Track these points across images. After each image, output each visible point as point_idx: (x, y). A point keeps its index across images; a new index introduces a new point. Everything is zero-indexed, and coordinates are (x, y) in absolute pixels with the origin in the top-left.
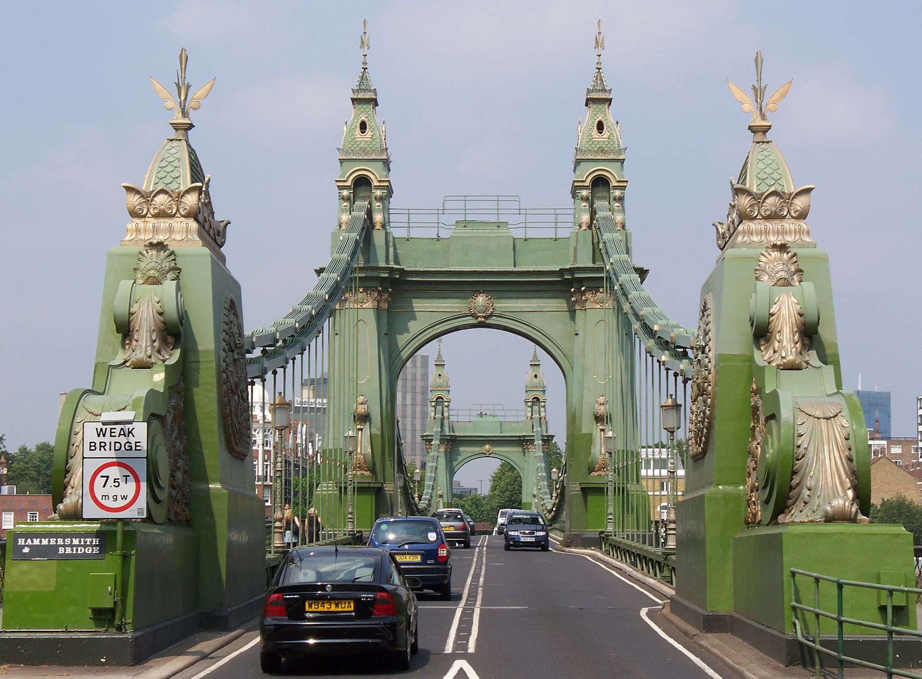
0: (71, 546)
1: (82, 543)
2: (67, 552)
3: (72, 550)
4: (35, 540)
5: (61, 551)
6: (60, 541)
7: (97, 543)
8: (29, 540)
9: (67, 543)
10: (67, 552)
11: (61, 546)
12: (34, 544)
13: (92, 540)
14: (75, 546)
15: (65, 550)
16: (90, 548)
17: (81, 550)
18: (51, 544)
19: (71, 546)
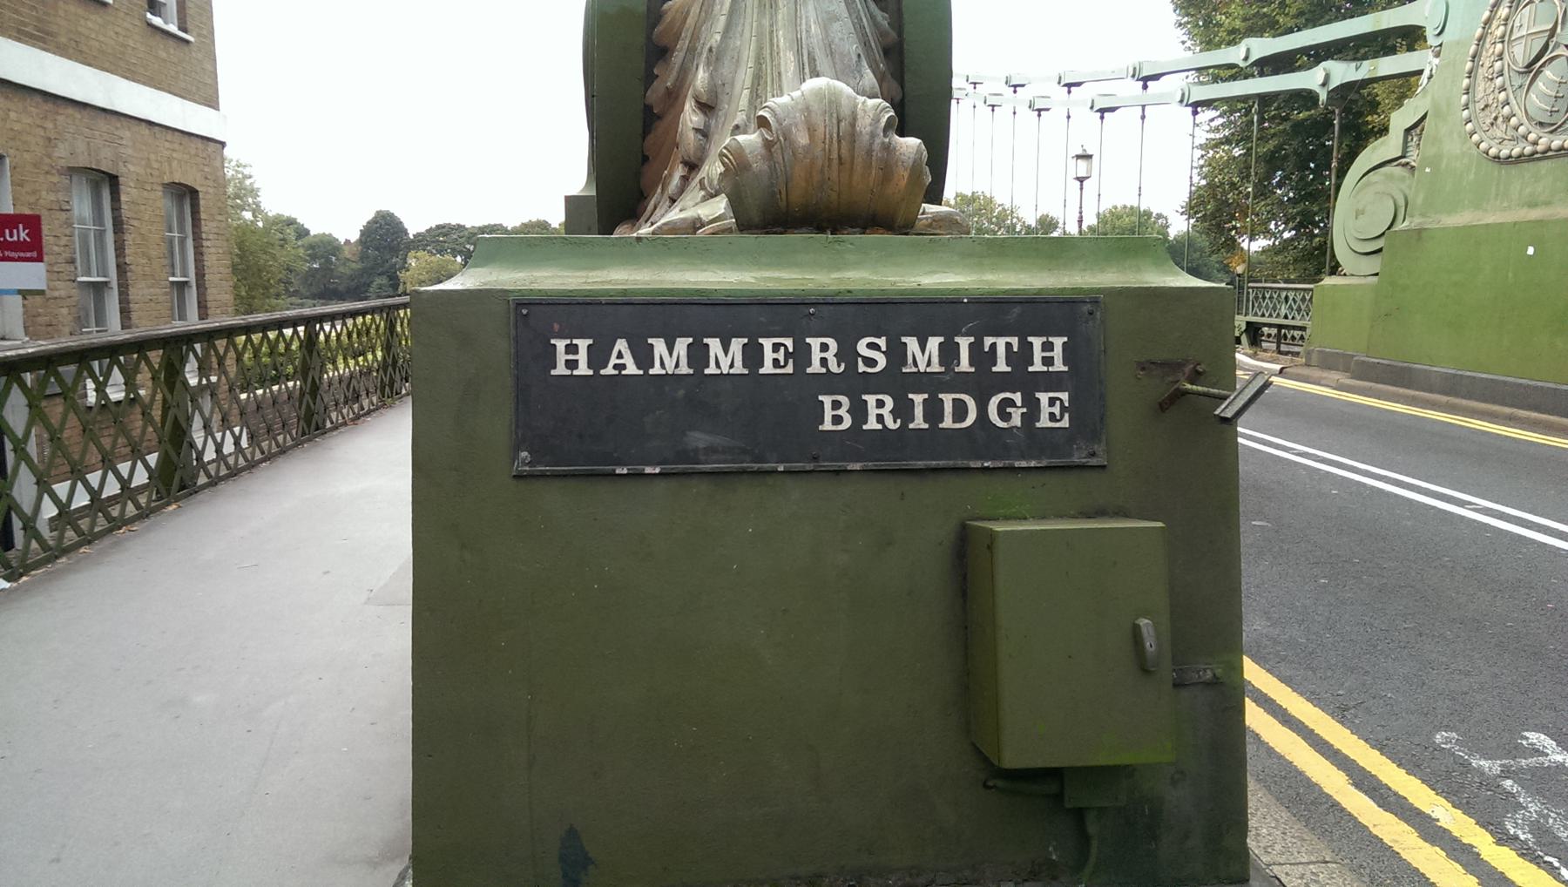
0: (897, 381)
1: (965, 365)
2: (872, 424)
3: (903, 410)
4: (659, 346)
5: (834, 414)
6: (823, 353)
7: (1059, 366)
8: (621, 345)
9: (871, 362)
10: (872, 424)
11: (828, 382)
12: (656, 370)
13: (1027, 348)
14: (923, 381)
15: (859, 411)
16: (1017, 397)
17: (960, 411)
18: (768, 368)
19: (897, 381)
